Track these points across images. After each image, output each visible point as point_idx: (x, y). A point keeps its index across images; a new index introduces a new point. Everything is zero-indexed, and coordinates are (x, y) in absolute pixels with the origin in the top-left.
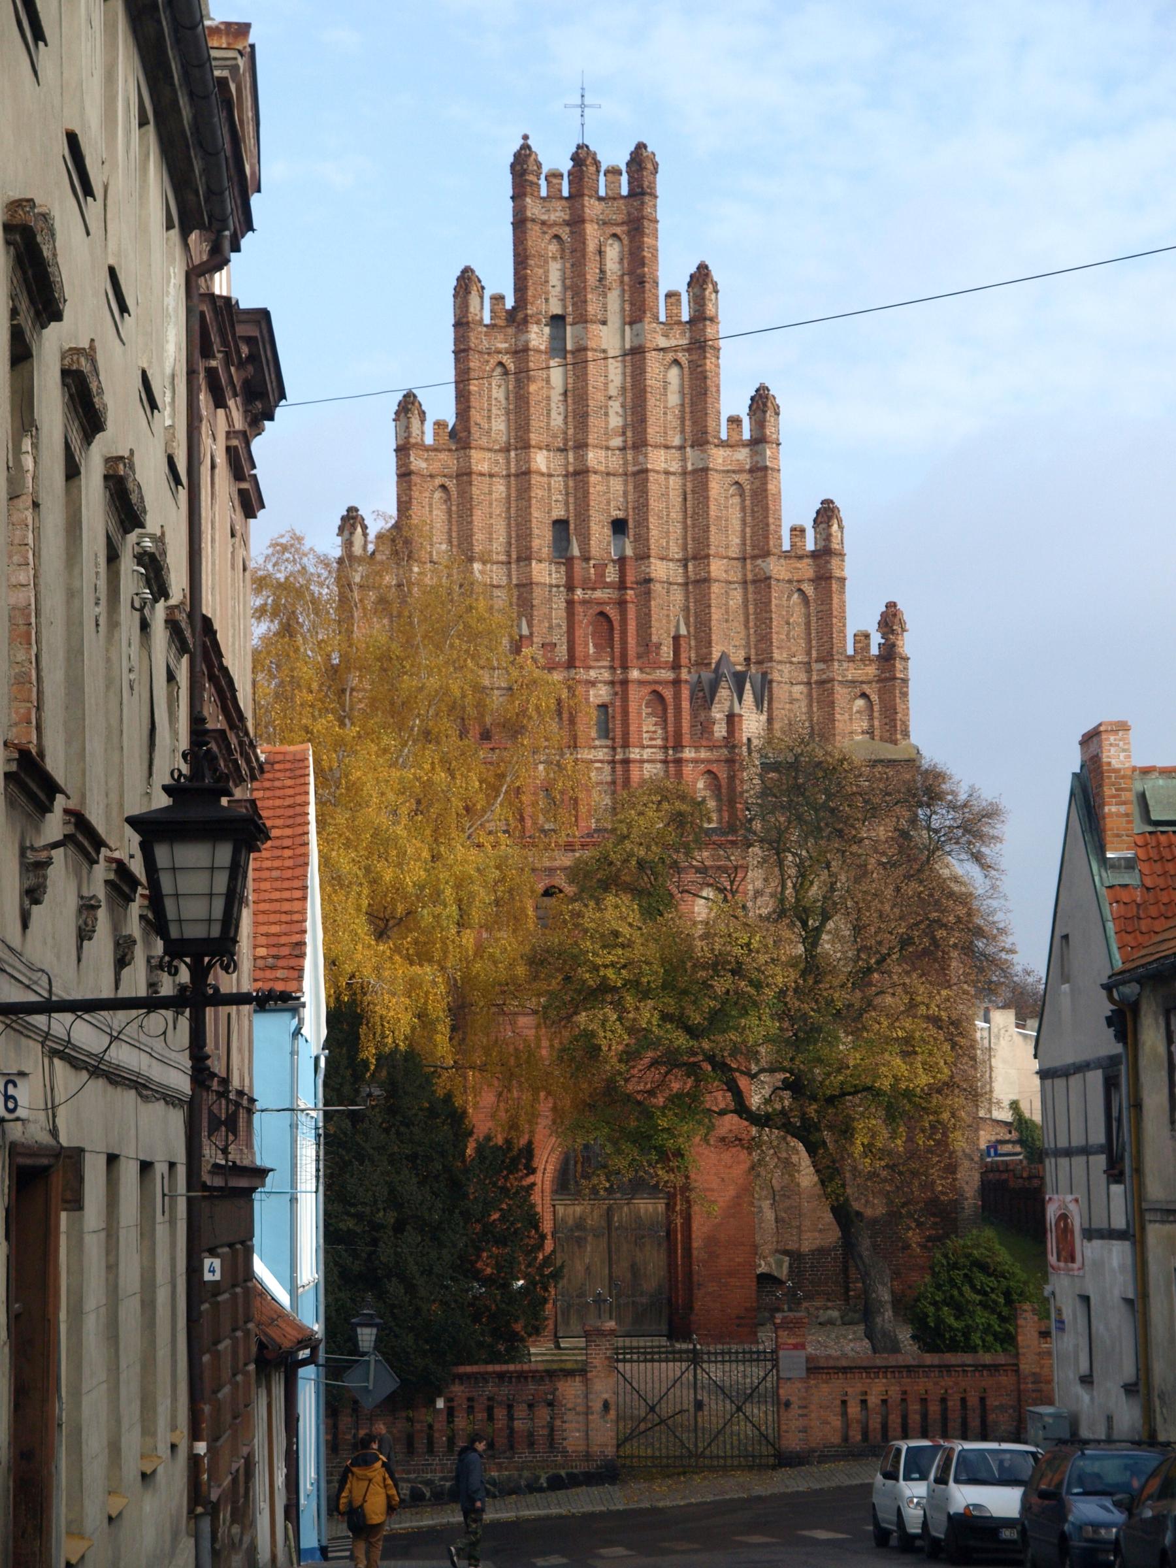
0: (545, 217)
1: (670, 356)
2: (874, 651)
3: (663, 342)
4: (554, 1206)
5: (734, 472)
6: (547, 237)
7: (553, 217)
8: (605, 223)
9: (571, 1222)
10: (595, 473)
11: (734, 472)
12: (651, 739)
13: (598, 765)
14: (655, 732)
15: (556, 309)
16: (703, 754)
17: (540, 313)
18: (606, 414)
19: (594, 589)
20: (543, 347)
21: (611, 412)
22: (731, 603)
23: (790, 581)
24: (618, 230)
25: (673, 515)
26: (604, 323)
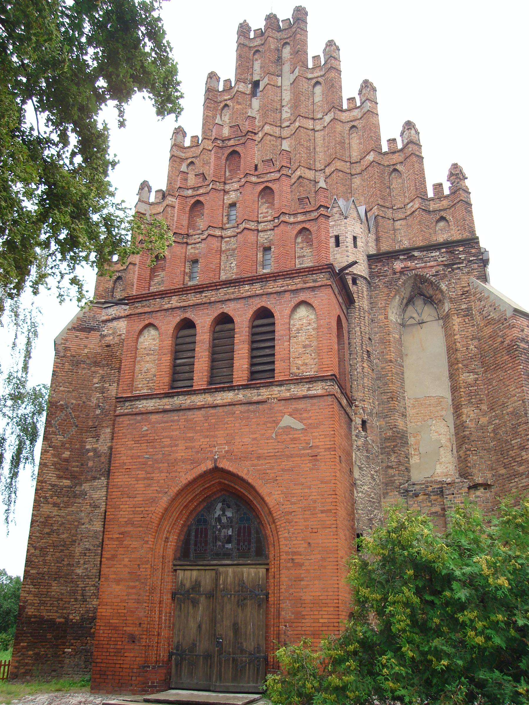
0: (251, 45)
1: (314, 81)
2: (447, 192)
3: (310, 76)
4: (175, 570)
5: (351, 121)
6: (253, 52)
7: (256, 44)
8: (281, 39)
9: (188, 585)
10: (271, 135)
11: (351, 121)
12: (264, 217)
13: (228, 239)
14: (267, 212)
15: (256, 78)
16: (300, 218)
17: (247, 79)
18: (281, 112)
19: (229, 139)
20: (248, 92)
21: (284, 112)
22: (353, 185)
23: (388, 166)
24: (288, 41)
25: (318, 149)
26: (280, 75)
